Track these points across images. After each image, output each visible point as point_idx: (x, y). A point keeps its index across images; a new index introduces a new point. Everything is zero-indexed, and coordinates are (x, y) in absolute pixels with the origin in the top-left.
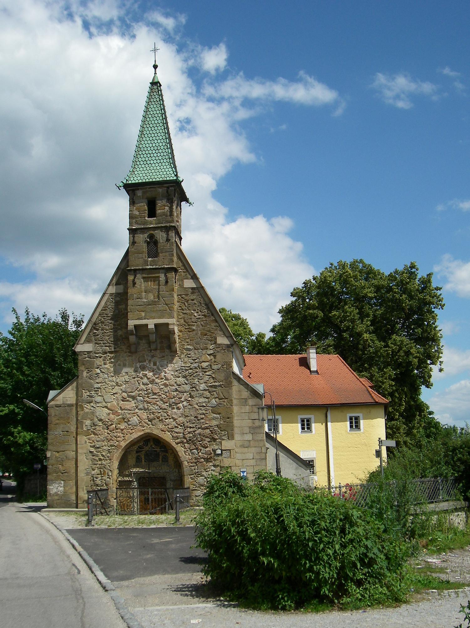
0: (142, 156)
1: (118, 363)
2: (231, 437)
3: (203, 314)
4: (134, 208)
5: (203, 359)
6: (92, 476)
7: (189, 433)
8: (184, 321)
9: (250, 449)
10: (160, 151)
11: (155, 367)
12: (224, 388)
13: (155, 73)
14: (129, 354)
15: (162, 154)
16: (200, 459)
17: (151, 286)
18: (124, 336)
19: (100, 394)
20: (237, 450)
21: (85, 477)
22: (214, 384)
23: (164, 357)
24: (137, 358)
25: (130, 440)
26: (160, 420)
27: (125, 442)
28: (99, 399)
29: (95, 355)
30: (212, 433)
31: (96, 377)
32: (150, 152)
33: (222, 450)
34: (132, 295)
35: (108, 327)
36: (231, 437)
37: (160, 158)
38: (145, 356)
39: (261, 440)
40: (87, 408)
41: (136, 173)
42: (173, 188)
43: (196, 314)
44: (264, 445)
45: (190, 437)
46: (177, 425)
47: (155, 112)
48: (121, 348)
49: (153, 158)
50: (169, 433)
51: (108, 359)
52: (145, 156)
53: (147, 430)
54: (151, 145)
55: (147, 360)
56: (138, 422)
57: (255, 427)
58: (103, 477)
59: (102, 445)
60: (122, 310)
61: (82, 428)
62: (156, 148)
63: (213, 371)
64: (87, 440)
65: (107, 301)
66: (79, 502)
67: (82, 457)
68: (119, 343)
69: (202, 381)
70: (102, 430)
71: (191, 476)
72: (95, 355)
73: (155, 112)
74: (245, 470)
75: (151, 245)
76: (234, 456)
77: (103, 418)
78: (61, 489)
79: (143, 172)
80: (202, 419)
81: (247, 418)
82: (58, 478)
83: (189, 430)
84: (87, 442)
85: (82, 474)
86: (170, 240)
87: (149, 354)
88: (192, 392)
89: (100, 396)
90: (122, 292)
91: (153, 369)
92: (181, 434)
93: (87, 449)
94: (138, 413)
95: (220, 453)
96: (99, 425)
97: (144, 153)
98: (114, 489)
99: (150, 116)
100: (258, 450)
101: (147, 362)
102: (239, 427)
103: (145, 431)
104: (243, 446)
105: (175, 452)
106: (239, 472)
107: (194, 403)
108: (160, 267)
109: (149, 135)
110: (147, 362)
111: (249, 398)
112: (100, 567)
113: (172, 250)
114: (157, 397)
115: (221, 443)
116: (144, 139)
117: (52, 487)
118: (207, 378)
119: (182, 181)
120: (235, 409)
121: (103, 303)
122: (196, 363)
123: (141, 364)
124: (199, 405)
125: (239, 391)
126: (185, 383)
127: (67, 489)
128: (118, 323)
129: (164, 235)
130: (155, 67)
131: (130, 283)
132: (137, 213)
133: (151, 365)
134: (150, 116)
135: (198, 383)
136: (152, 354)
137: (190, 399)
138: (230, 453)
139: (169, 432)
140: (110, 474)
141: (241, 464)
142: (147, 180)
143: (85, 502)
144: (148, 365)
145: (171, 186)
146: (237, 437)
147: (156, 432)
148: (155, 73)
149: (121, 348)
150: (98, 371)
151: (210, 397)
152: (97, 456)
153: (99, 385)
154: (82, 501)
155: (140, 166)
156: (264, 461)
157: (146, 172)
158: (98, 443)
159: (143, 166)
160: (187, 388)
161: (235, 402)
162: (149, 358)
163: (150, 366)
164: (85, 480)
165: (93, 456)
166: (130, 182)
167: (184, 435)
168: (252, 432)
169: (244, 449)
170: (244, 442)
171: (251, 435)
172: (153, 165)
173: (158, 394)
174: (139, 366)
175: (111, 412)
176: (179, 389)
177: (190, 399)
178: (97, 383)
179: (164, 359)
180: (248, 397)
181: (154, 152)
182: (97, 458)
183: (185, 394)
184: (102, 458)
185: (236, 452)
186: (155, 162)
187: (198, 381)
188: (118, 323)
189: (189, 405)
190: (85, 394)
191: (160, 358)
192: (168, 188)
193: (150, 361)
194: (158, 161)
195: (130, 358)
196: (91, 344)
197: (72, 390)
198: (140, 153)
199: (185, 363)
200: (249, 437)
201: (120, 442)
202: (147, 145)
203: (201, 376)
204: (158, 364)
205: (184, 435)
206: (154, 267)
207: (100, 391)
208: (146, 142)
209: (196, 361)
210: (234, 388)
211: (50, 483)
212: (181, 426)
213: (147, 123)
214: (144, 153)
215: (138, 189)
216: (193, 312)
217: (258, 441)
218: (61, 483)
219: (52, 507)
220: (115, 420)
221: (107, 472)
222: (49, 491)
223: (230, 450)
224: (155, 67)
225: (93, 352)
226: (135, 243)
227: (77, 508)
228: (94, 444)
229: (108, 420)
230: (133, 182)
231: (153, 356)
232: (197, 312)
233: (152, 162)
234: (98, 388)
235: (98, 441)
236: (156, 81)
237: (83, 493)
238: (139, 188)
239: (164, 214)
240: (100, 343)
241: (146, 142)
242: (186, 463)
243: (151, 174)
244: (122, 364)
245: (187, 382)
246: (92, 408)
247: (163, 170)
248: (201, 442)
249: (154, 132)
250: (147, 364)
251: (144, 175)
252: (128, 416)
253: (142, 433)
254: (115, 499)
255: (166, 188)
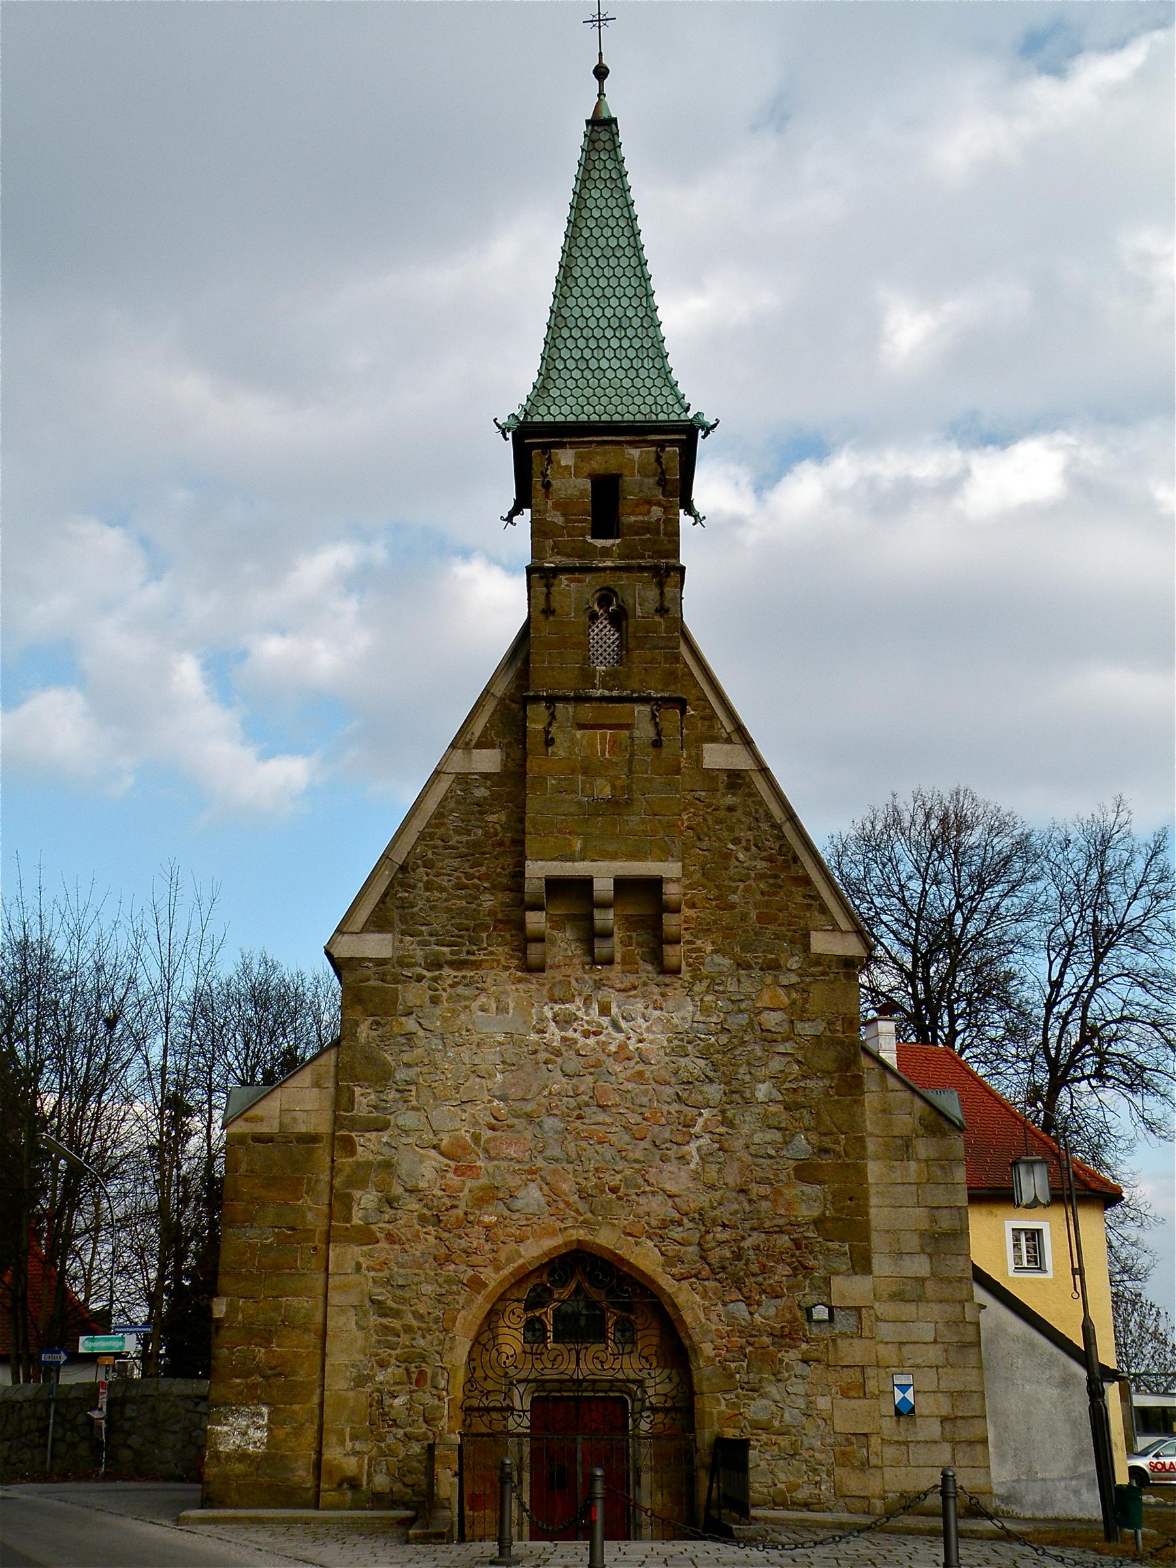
0: (570, 343)
1: (478, 1003)
2: (862, 1264)
3: (765, 854)
4: (550, 503)
5: (766, 1000)
6: (378, 1390)
7: (720, 1243)
8: (704, 874)
9: (923, 1307)
10: (631, 332)
11: (605, 1021)
12: (836, 1098)
13: (601, 94)
14: (519, 974)
15: (637, 343)
16: (755, 1336)
17: (603, 754)
18: (500, 916)
19: (414, 1103)
20: (880, 1308)
21: (351, 1394)
22: (801, 1084)
23: (634, 988)
24: (547, 987)
25: (516, 1265)
26: (620, 1198)
27: (497, 1269)
28: (408, 1119)
29: (398, 970)
30: (798, 1247)
31: (403, 1045)
32: (598, 333)
33: (831, 1310)
34: (542, 779)
35: (450, 881)
36: (862, 1264)
37: (631, 353)
38: (574, 983)
39: (960, 1280)
40: (368, 1146)
41: (555, 393)
42: (677, 449)
43: (741, 856)
44: (971, 1298)
45: (722, 1259)
46: (677, 1216)
47: (606, 213)
48: (492, 953)
49: (609, 353)
50: (652, 1244)
51: (446, 986)
52: (582, 343)
53: (574, 1232)
54: (598, 312)
55: (580, 995)
56: (543, 1200)
57: (940, 1234)
58: (415, 1391)
59: (416, 1279)
60: (495, 829)
61: (348, 1219)
62: (615, 323)
63: (798, 1039)
64: (361, 1260)
65: (445, 798)
66: (323, 1486)
67: (342, 1320)
68: (484, 935)
69: (762, 1072)
70: (418, 1227)
71: (727, 1396)
72: (398, 970)
73: (606, 213)
74: (907, 1380)
75: (601, 626)
76: (871, 1331)
77: (423, 1185)
78: (259, 1434)
79: (577, 392)
80: (765, 1198)
81: (912, 1200)
82: (252, 1396)
83: (718, 1236)
84: (364, 1266)
85: (338, 1384)
86: (667, 611)
87: (586, 976)
88: (728, 1106)
89: (413, 1109)
90: (498, 771)
91: (599, 1025)
92: (691, 1249)
93: (362, 1292)
94: (542, 1173)
95: (826, 1317)
96: (410, 1207)
97: (576, 333)
98: (453, 1436)
99: (591, 223)
100: (952, 1311)
101: (579, 1002)
102: (888, 1231)
103: (568, 1232)
104: (898, 1297)
105: (669, 1309)
106: (890, 1389)
107: (736, 1144)
108: (635, 695)
109: (592, 282)
110: (579, 1002)
111: (917, 1136)
112: (647, 1531)
113: (674, 644)
114: (609, 1120)
115: (827, 1281)
116: (576, 292)
117: (226, 1428)
118: (776, 1064)
119: (714, 426)
120: (874, 1170)
121: (431, 805)
122: (741, 1011)
123: (557, 1007)
124: (754, 1152)
125: (884, 1111)
126: (707, 1076)
127: (280, 1434)
128: (483, 869)
129: (652, 594)
130: (601, 73)
131: (534, 741)
132: (560, 520)
133: (592, 1012)
134: (591, 223)
135: (747, 1078)
136: (597, 978)
137: (722, 1130)
138: (860, 1318)
139: (649, 1237)
140: (443, 1384)
141: (894, 1360)
142: (594, 418)
143: (345, 1486)
144: (580, 1014)
145: (672, 443)
146: (881, 1264)
147: (606, 1238)
148: (601, 94)
149: (492, 953)
150: (410, 1024)
151: (790, 1127)
152: (397, 1314)
153: (411, 1073)
154: (337, 1479)
155: (565, 374)
156: (973, 1351)
157: (588, 392)
158: (401, 1271)
159: (576, 374)
160: (714, 1092)
161: (872, 1146)
162: (587, 991)
163: (588, 1016)
164: (351, 1403)
165: (385, 1316)
166: (537, 419)
167: (703, 1250)
168: (928, 1250)
169: (902, 1305)
170: (904, 1284)
171: (924, 1259)
172: (610, 374)
173: (614, 1110)
174: (550, 1015)
175: (452, 1164)
176: (684, 1095)
177: (722, 1130)
178: (408, 1065)
179: (635, 997)
180: (914, 1130)
181: (609, 333)
182: (396, 1324)
183: (706, 1113)
184: (415, 1323)
185: (878, 1319)
186: (615, 364)
187: (750, 1073)
188: (483, 869)
189: (720, 1149)
190: (364, 1099)
191: (624, 990)
192: (661, 445)
193: (587, 1001)
194: (626, 364)
195: (520, 986)
196: (389, 936)
197: (317, 1084)
198: (565, 333)
199: (706, 1010)
200: (919, 1266)
201: (481, 1269)
202: (587, 312)
203: (759, 1054)
204: (614, 1010)
205: (703, 1250)
206: (615, 693)
207: (413, 1093)
208: (582, 302)
209: (743, 1006)
210: (868, 1098)
211: (219, 1412)
212: (692, 1220)
213: (581, 242)
214: (576, 333)
215: (562, 445)
216: (730, 846)
217: (948, 1280)
218: (261, 1415)
219: (222, 1505)
220: (466, 1191)
221: (429, 1375)
222: (216, 1444)
223: (858, 1309)
224: (601, 73)
225: (395, 960)
226: (553, 612)
227: (317, 1507)
228: (386, 1273)
229: (440, 1193)
230: (548, 418)
231: (599, 985)
232: (747, 849)
233: (604, 364)
234: (408, 1083)
235: (402, 1266)
236: (605, 115)
237: (339, 1450)
238: (565, 440)
239: (646, 528)
240: (421, 933)
241: (582, 302)
242: (708, 1349)
243: (604, 400)
244: (494, 1006)
245: (711, 1074)
246: (386, 1150)
247: (644, 392)
248: (760, 1279)
249: (608, 272)
250: (579, 1009)
251: (582, 401)
252: (513, 1181)
253: (558, 1241)
254: (456, 1475)
255: (654, 449)
